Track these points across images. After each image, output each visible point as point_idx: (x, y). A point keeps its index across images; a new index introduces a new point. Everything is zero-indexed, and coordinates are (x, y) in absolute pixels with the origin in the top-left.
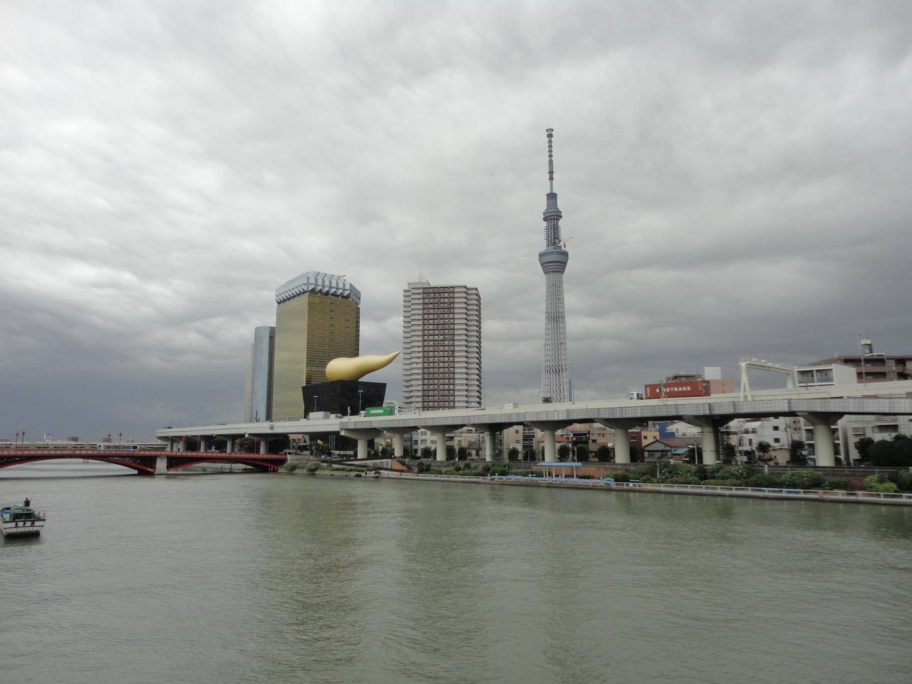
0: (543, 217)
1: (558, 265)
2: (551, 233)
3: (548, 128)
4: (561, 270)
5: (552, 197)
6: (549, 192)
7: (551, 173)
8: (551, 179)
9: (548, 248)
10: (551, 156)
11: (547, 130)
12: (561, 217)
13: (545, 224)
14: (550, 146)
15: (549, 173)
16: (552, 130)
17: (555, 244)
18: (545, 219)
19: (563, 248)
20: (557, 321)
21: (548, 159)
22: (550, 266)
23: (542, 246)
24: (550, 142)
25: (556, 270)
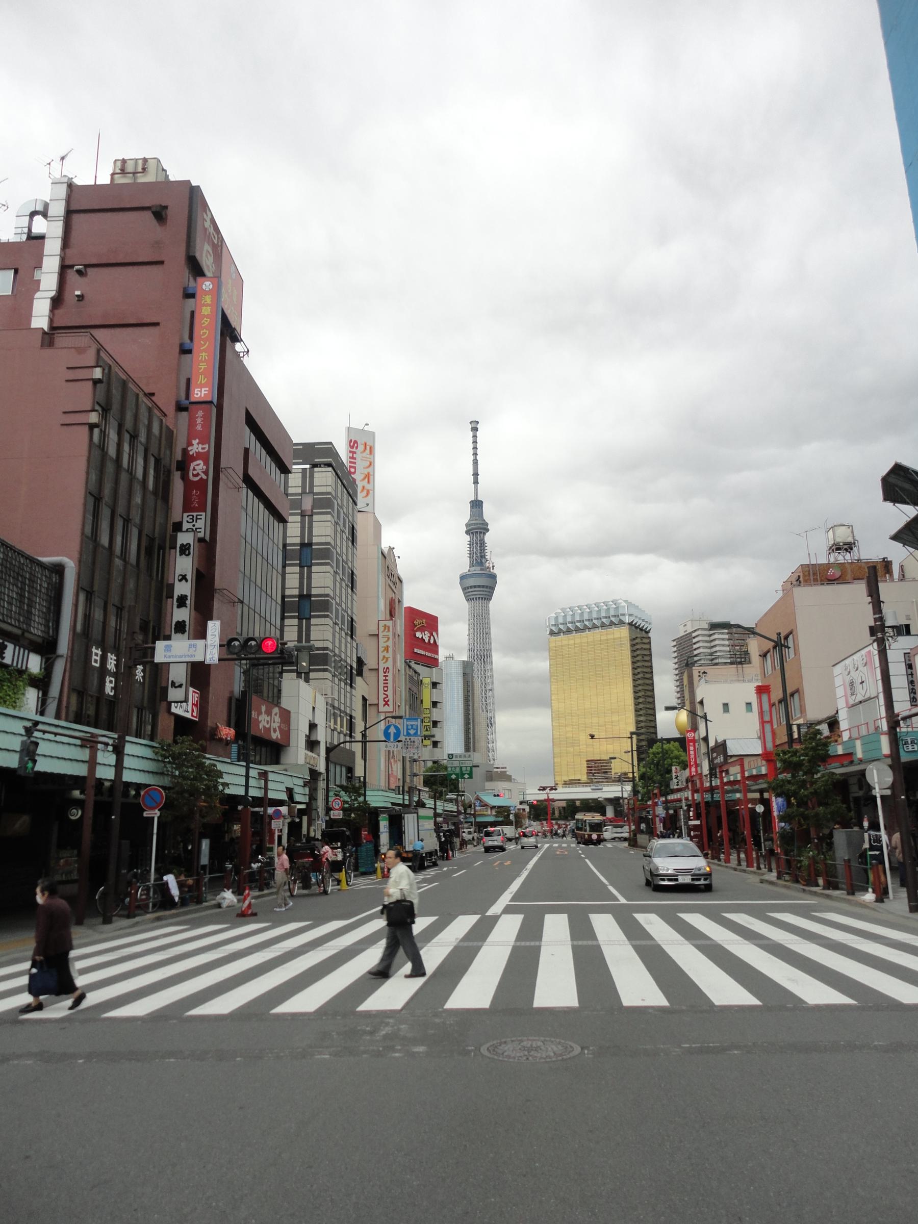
0: (465, 529)
1: (486, 591)
2: (477, 550)
3: (474, 420)
4: (486, 597)
5: (477, 505)
6: (473, 499)
7: (476, 475)
8: (476, 482)
9: (473, 569)
10: (475, 454)
11: (471, 423)
12: (488, 530)
13: (468, 538)
14: (475, 442)
15: (473, 475)
16: (478, 422)
17: (481, 564)
18: (467, 532)
19: (492, 570)
20: (484, 662)
21: (472, 458)
22: (475, 591)
23: (464, 565)
24: (475, 436)
25: (481, 596)
